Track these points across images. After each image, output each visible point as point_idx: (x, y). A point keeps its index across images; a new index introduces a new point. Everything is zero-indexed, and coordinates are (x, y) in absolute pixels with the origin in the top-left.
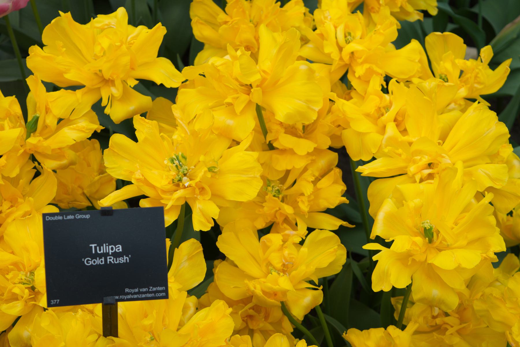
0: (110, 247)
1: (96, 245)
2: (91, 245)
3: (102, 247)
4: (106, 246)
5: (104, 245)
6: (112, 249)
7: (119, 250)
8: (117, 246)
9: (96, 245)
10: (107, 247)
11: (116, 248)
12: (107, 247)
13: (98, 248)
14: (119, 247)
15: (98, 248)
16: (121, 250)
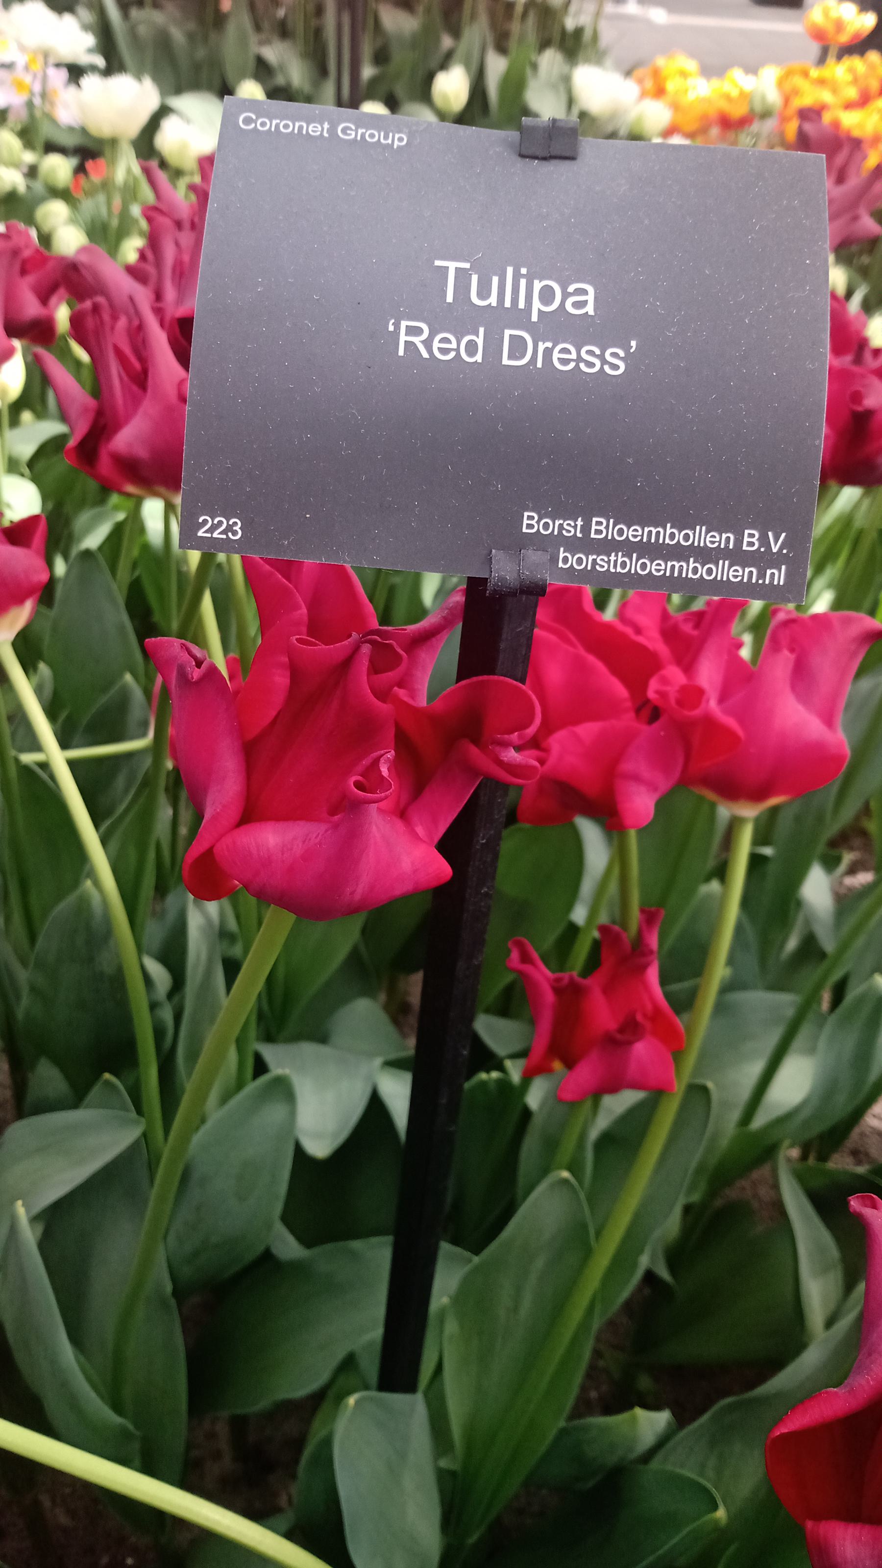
0: (538, 285)
1: (467, 265)
2: (438, 263)
3: (495, 280)
4: (517, 277)
5: (510, 270)
6: (547, 295)
7: (576, 305)
8: (571, 289)
9: (467, 265)
10: (523, 282)
11: (566, 295)
12: (523, 282)
13: (475, 278)
14: (584, 292)
15: (475, 278)
16: (590, 309)
